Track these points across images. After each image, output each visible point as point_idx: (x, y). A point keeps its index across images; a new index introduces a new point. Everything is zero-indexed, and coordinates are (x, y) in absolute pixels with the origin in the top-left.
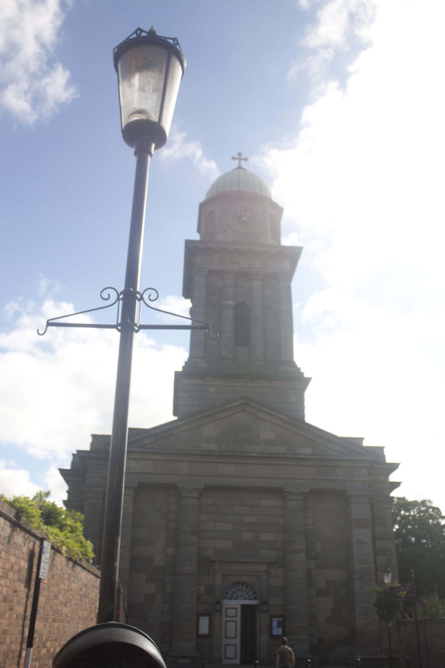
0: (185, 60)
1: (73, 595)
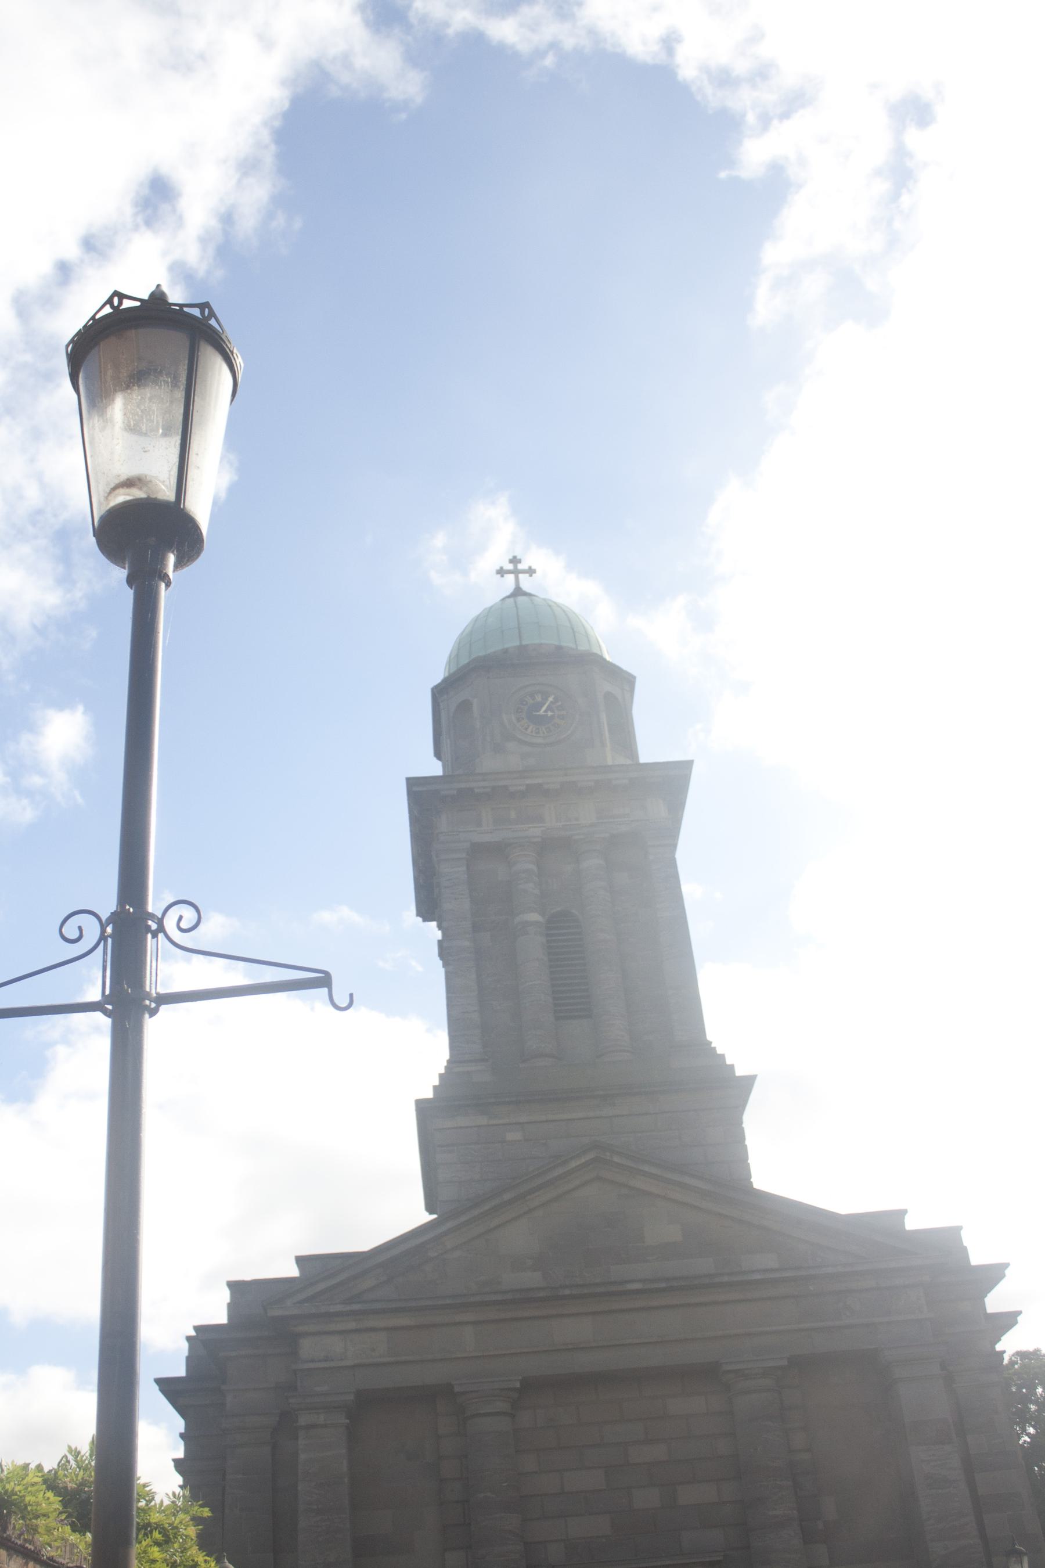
0: (235, 351)
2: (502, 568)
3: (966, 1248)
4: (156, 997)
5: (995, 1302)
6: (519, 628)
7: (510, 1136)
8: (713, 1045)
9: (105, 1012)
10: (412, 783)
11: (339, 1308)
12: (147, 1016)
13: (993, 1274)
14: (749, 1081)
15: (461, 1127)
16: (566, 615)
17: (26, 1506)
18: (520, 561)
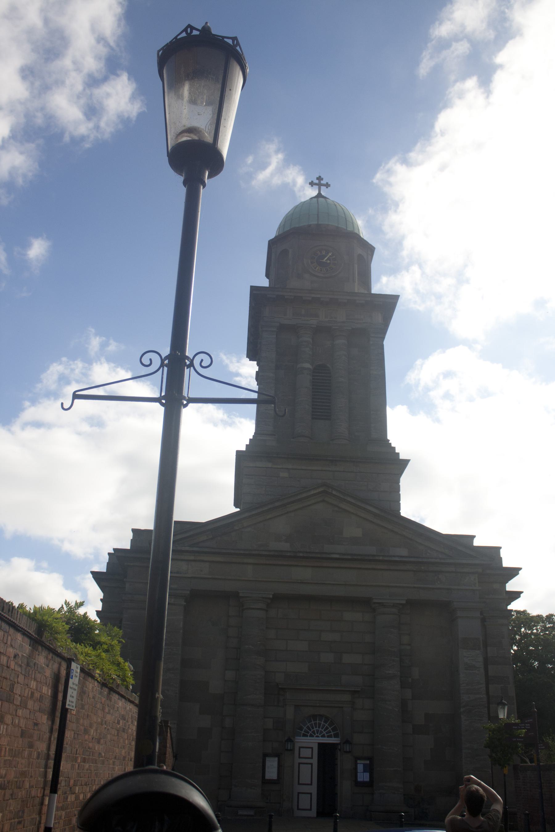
0: (247, 65)
1: (108, 729)
2: (312, 181)
3: (501, 558)
4: (188, 399)
5: (511, 586)
6: (318, 215)
8: (390, 442)
9: (162, 404)
10: (253, 289)
11: (187, 548)
13: (514, 572)
14: (406, 462)
16: (344, 211)
18: (322, 179)
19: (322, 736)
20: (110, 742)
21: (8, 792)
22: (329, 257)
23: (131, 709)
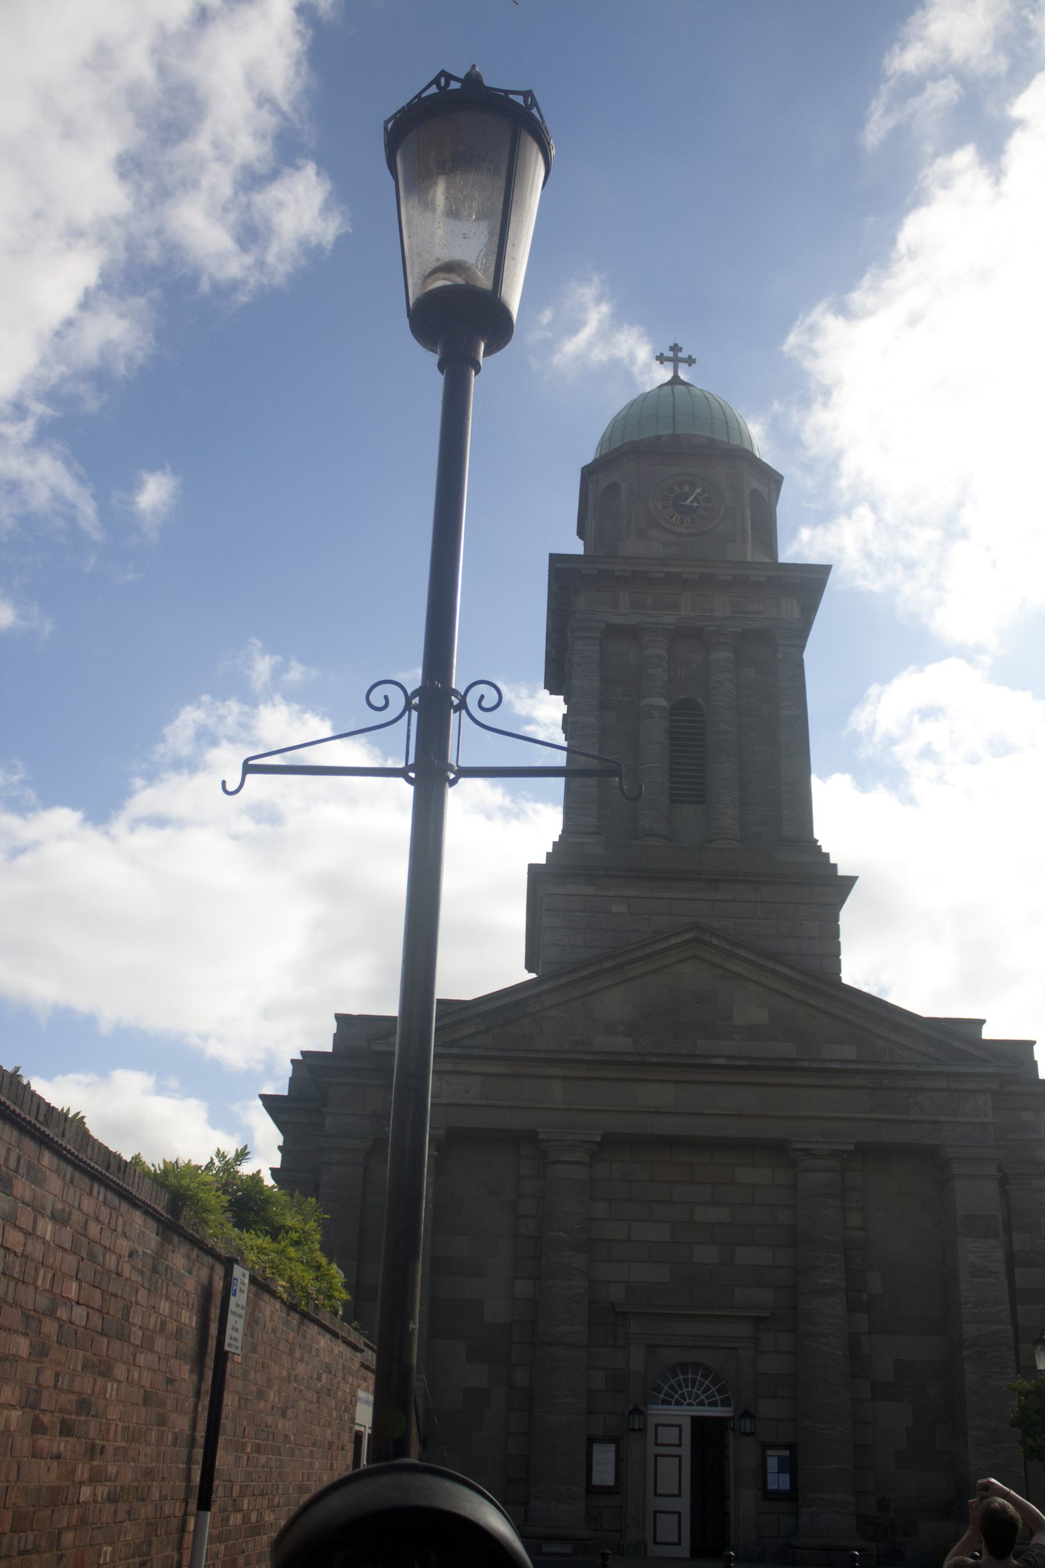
0: (551, 142)
1: (300, 1391)
2: (662, 354)
3: (1036, 1062)
6: (674, 417)
7: (615, 908)
8: (819, 844)
9: (410, 781)
12: (447, 785)
14: (850, 881)
15: (570, 895)
16: (722, 409)
17: (198, 1201)
18: (680, 350)
19: (698, 1404)
20: (304, 1414)
21: (123, 1507)
22: (695, 497)
23: (342, 1352)
